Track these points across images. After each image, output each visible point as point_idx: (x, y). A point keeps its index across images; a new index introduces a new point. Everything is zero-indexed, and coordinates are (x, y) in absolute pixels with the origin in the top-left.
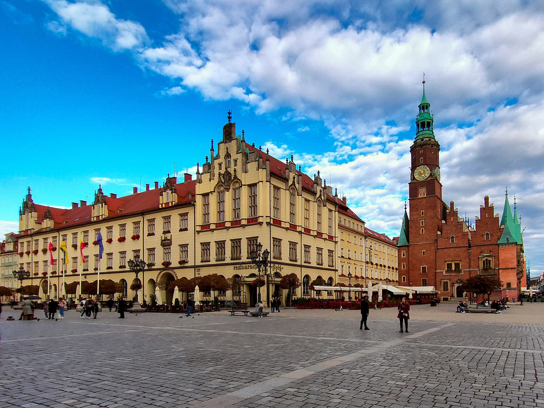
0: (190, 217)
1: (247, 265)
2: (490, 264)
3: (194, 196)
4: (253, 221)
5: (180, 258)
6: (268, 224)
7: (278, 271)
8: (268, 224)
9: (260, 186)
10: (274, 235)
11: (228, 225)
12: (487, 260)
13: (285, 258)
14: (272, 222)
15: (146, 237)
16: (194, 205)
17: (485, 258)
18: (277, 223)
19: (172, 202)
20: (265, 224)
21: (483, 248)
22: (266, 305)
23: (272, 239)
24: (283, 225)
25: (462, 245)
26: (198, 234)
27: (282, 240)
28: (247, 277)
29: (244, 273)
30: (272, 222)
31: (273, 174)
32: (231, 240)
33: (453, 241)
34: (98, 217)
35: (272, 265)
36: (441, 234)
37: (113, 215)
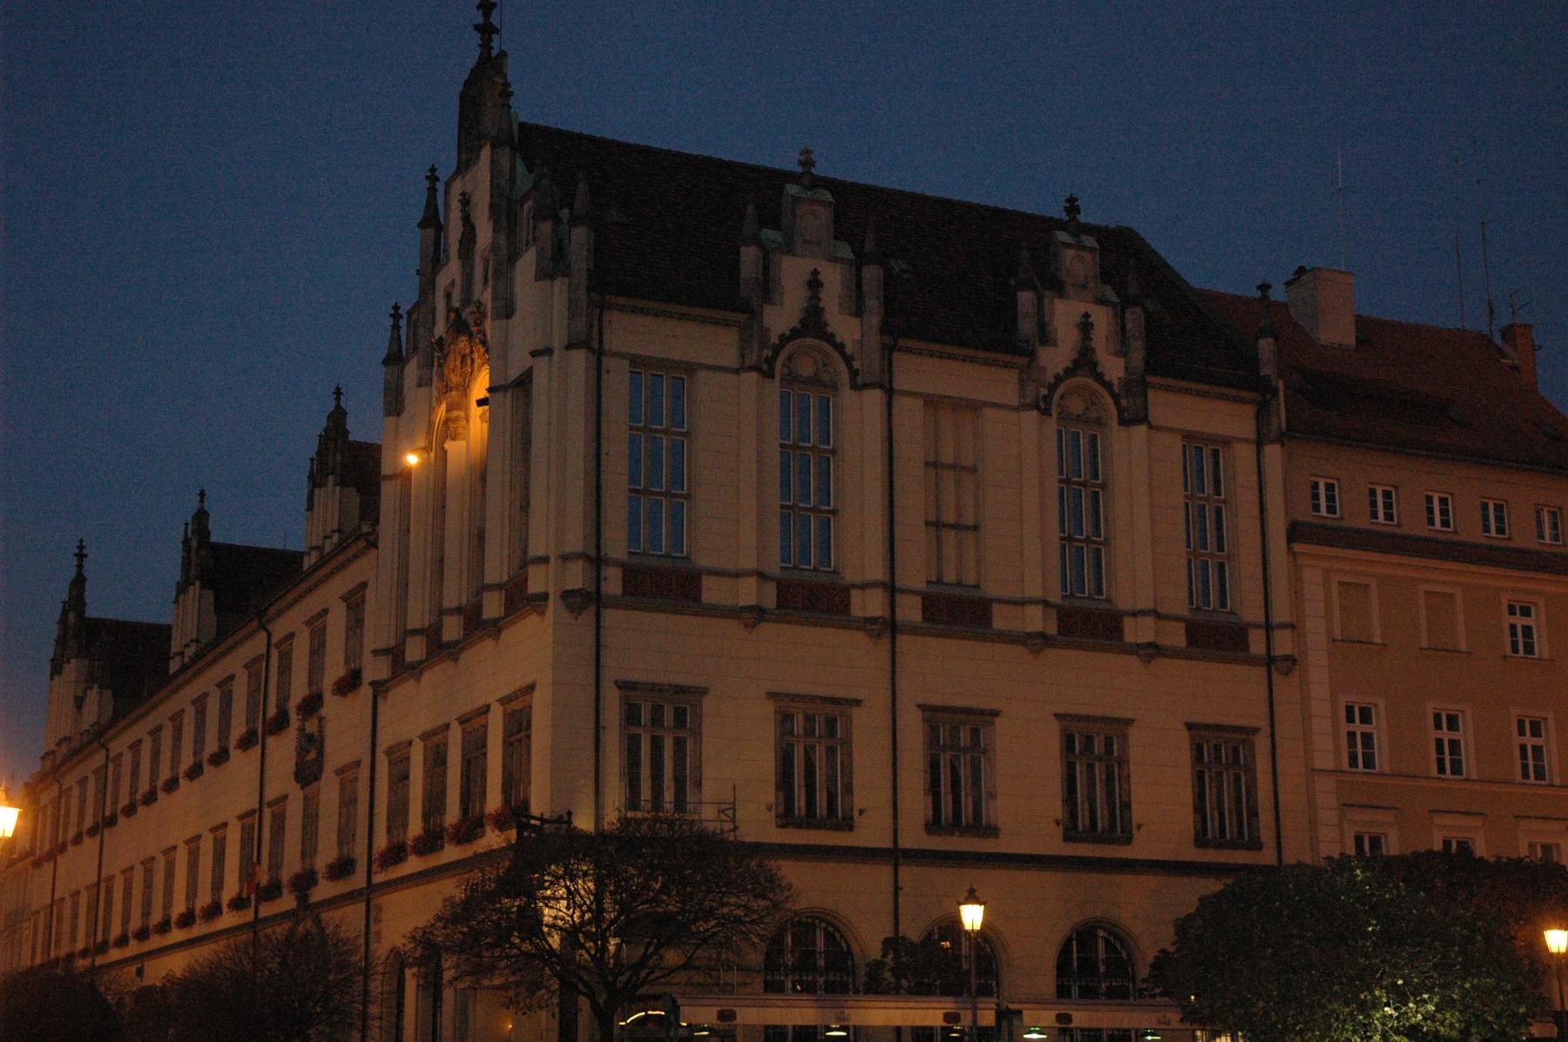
6: (587, 601)
8: (587, 601)
18: (668, 585)
27: (704, 691)
34: (181, 654)
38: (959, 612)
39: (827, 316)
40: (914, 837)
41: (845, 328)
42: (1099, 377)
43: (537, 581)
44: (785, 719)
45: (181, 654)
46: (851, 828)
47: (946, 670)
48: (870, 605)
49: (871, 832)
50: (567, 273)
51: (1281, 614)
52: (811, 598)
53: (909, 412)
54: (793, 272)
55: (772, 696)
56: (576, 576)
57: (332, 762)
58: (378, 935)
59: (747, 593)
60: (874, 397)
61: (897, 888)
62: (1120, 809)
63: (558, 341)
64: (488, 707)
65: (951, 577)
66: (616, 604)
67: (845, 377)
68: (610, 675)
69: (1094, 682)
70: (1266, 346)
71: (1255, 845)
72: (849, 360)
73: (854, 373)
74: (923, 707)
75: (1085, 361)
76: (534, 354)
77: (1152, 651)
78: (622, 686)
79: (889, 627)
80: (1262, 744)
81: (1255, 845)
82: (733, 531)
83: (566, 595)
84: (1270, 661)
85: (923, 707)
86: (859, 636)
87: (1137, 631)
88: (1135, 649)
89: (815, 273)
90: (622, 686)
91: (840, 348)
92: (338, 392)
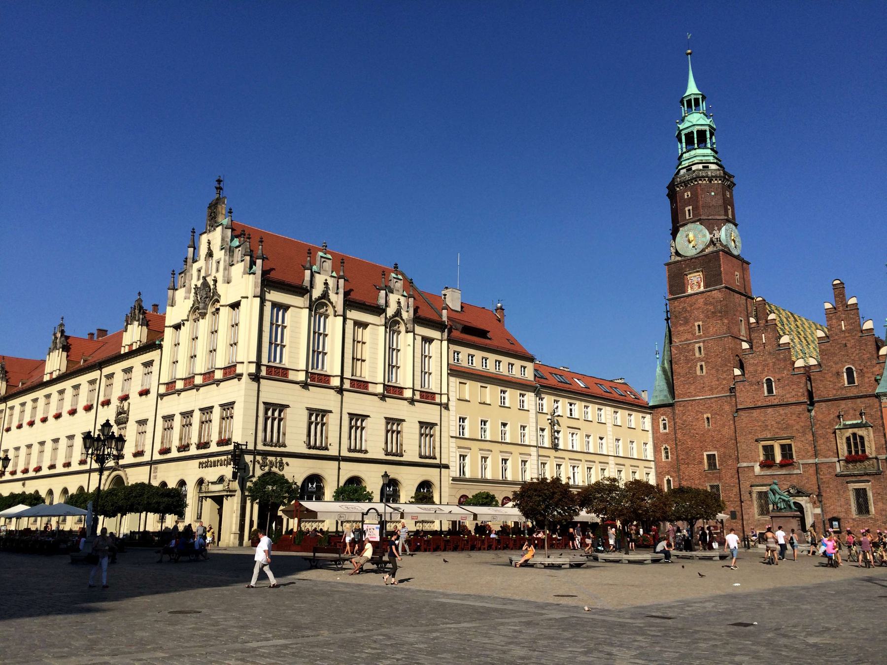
0: (155, 368)
1: (216, 459)
2: (863, 445)
4: (231, 373)
5: (136, 446)
6: (256, 377)
7: (274, 469)
8: (256, 377)
9: (244, 302)
10: (266, 397)
11: (198, 380)
12: (854, 435)
13: (295, 440)
15: (100, 407)
16: (160, 347)
17: (850, 431)
18: (280, 374)
20: (245, 378)
21: (843, 405)
22: (237, 542)
23: (262, 407)
24: (292, 376)
25: (793, 400)
26: (161, 399)
28: (213, 483)
30: (264, 373)
31: (268, 282)
32: (201, 410)
33: (770, 391)
34: (51, 373)
35: (259, 458)
36: (743, 374)
37: (76, 367)
38: (360, 386)
40: (345, 453)
41: (333, 297)
43: (239, 369)
44: (311, 415)
45: (51, 373)
47: (355, 403)
48: (336, 382)
49: (333, 451)
50: (254, 274)
51: (444, 391)
53: (350, 324)
54: (319, 280)
55: (308, 409)
56: (252, 369)
57: (133, 417)
58: (155, 477)
59: (301, 377)
60: (340, 320)
61: (339, 468)
62: (400, 445)
63: (250, 295)
64: (212, 407)
65: (358, 374)
67: (332, 312)
68: (261, 400)
69: (395, 408)
70: (445, 312)
71: (435, 458)
72: (334, 307)
73: (335, 312)
75: (398, 313)
76: (243, 297)
77: (412, 401)
78: (264, 403)
79: (340, 390)
80: (437, 428)
81: (435, 458)
83: (250, 375)
84: (440, 404)
87: (408, 394)
90: (264, 403)
91: (332, 303)
92: (140, 294)
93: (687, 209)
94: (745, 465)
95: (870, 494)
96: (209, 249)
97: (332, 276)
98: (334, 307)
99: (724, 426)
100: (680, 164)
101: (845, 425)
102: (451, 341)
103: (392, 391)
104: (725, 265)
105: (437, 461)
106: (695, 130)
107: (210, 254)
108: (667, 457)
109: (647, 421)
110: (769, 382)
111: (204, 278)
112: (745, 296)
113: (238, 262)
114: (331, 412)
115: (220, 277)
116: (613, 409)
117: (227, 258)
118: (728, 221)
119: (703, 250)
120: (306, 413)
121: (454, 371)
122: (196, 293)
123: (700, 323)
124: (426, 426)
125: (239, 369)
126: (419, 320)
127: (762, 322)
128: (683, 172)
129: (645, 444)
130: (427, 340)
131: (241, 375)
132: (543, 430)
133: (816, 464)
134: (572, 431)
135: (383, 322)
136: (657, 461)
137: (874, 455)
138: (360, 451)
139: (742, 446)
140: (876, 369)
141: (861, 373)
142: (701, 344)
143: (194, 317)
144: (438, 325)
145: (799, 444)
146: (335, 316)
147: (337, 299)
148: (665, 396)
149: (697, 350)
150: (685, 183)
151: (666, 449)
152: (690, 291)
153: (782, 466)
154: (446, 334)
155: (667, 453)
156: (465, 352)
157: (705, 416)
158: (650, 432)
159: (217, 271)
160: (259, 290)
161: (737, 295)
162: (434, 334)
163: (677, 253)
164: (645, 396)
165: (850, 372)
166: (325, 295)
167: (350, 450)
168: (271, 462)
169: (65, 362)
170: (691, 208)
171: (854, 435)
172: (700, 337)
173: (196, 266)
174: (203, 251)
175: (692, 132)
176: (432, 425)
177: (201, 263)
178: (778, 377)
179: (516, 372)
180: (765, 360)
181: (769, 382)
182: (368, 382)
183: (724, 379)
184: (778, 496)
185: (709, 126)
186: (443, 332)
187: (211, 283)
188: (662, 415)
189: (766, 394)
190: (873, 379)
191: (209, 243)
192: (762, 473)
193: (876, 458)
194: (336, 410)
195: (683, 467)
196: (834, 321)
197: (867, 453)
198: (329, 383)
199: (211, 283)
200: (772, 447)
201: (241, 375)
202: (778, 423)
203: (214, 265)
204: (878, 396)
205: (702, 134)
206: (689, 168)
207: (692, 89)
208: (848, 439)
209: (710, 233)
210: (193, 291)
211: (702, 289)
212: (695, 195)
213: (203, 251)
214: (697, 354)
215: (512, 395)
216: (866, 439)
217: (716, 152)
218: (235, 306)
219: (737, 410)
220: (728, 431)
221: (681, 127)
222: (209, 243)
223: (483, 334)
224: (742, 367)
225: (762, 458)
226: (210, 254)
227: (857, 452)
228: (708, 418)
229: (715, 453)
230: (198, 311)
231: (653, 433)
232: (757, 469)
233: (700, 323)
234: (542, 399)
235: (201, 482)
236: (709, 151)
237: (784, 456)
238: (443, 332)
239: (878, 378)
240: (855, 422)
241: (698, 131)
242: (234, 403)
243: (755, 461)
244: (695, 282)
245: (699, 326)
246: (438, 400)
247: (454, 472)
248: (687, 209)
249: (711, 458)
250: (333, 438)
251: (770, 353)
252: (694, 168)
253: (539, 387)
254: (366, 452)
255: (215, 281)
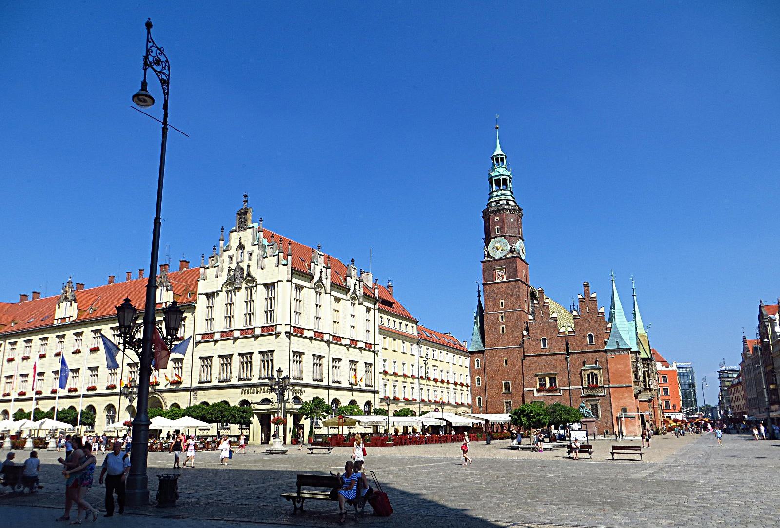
2: (597, 379)
3: (194, 293)
4: (270, 330)
6: (288, 335)
7: (298, 395)
12: (592, 373)
14: (292, 332)
16: (194, 308)
17: (590, 371)
18: (298, 332)
19: (166, 303)
20: (283, 335)
23: (292, 354)
24: (306, 333)
28: (258, 404)
29: (255, 398)
30: (292, 332)
31: (295, 272)
33: (545, 345)
36: (529, 335)
39: (323, 279)
40: (331, 384)
41: (324, 281)
42: (356, 295)
46: (323, 381)
47: (336, 351)
49: (325, 383)
52: (318, 336)
56: (287, 329)
61: (328, 394)
66: (293, 335)
69: (354, 354)
71: (372, 387)
73: (325, 290)
74: (332, 358)
75: (355, 292)
77: (361, 349)
78: (293, 351)
79: (328, 343)
80: (373, 367)
82: (282, 317)
85: (332, 358)
86: (324, 343)
88: (358, 348)
89: (321, 270)
90: (293, 351)
93: (496, 228)
94: (528, 389)
95: (599, 407)
96: (240, 243)
97: (324, 267)
98: (324, 287)
99: (515, 365)
100: (491, 198)
101: (587, 367)
102: (380, 311)
103: (353, 343)
104: (520, 265)
105: (373, 388)
106: (501, 177)
107: (241, 247)
108: (479, 384)
109: (465, 361)
110: (544, 339)
111: (238, 263)
112: (527, 285)
113: (270, 256)
114: (324, 357)
115: (254, 263)
116: (452, 354)
117: (260, 252)
118: (520, 238)
119: (506, 255)
120: (312, 357)
121: (384, 332)
122: (229, 273)
123: (503, 301)
124: (368, 365)
125: (279, 329)
126: (366, 296)
127: (541, 303)
128: (493, 204)
129: (466, 376)
130: (368, 310)
131: (280, 333)
132: (421, 367)
133: (569, 389)
134: (434, 368)
135: (348, 297)
136: (473, 387)
137: (602, 385)
138: (337, 382)
139: (526, 378)
140: (605, 335)
141: (597, 337)
142: (503, 314)
143: (226, 289)
144: (375, 301)
145: (561, 378)
146: (325, 294)
147: (327, 283)
148: (479, 346)
149: (500, 317)
150: (496, 212)
151: (478, 379)
152: (497, 281)
153: (550, 390)
154: (377, 307)
155: (478, 381)
156: (385, 317)
157: (504, 359)
158: (469, 368)
159: (250, 260)
160: (290, 276)
161: (524, 285)
162: (372, 306)
163: (489, 255)
164: (465, 345)
165: (591, 336)
166: (320, 280)
167: (333, 382)
168: (297, 390)
169: (76, 311)
170: (499, 227)
171: (592, 373)
172: (503, 309)
173: (226, 254)
174: (234, 244)
175: (500, 179)
176: (371, 365)
177: (233, 251)
178: (549, 337)
179: (410, 330)
180: (542, 327)
181: (544, 339)
182: (341, 337)
183: (517, 337)
184: (585, 410)
185: (509, 176)
186: (375, 304)
187: (245, 268)
188: (477, 357)
189: (542, 347)
190: (603, 341)
191: (240, 239)
192: (538, 394)
193: (604, 387)
194: (326, 356)
195: (488, 391)
196: (583, 306)
197: (599, 384)
198: (323, 338)
199: (245, 268)
200: (544, 380)
201: (280, 333)
202: (548, 364)
203: (246, 255)
204: (605, 351)
205: (505, 181)
206: (497, 202)
207: (498, 151)
208: (589, 375)
209: (511, 245)
210: (226, 271)
211: (505, 280)
212: (502, 219)
213: (234, 244)
214: (500, 320)
215: (407, 344)
216: (598, 375)
217: (512, 193)
218: (269, 286)
219: (524, 357)
220: (518, 369)
221: (493, 174)
222: (240, 239)
223: (390, 304)
224: (527, 329)
225: (538, 386)
226: (241, 247)
227: (593, 383)
228: (506, 360)
229: (510, 382)
230: (232, 284)
231: (471, 369)
232: (535, 393)
233: (503, 301)
234: (421, 347)
235: (245, 402)
236: (509, 193)
237: (551, 384)
238: (375, 304)
239: (607, 340)
240: (592, 366)
241: (503, 179)
242: (274, 351)
243: (534, 387)
244: (500, 276)
245: (502, 302)
246: (373, 349)
247: (381, 395)
248: (496, 228)
249: (507, 384)
250: (325, 375)
251: (545, 323)
252: (501, 202)
253: (418, 341)
254: (340, 383)
255: (249, 266)
